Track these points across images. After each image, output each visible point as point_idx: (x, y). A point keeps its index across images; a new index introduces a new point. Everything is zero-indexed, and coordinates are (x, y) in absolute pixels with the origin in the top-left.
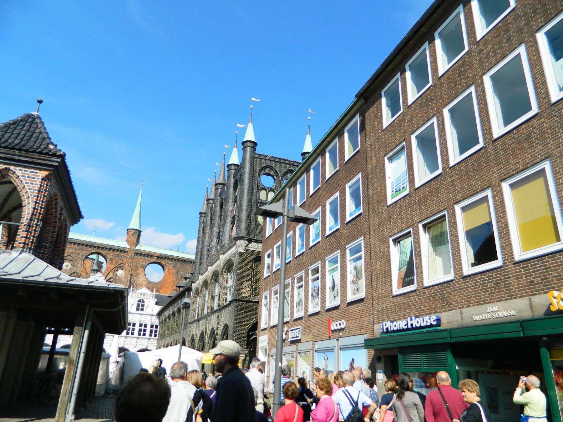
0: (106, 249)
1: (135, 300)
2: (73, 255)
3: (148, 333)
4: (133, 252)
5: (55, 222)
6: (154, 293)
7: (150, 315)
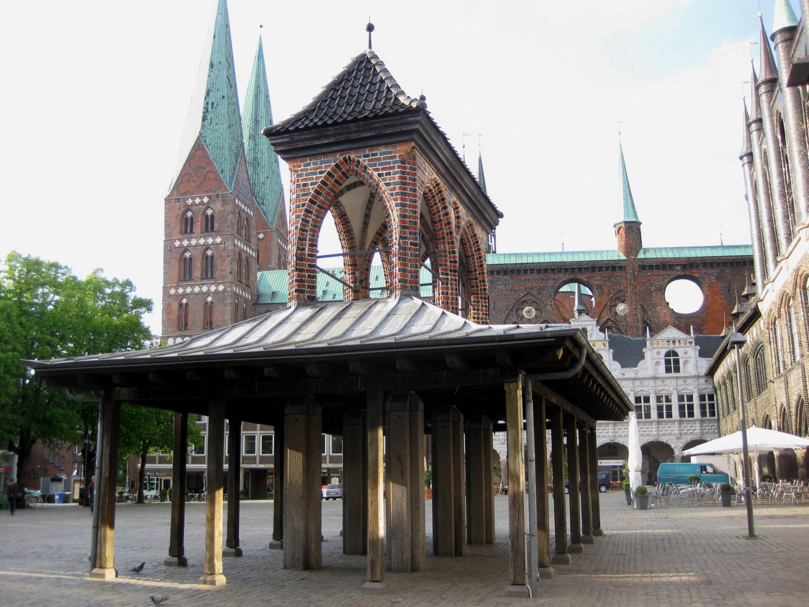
0: (587, 269)
1: (658, 353)
2: (534, 292)
3: (697, 411)
4: (636, 266)
5: (451, 233)
6: (692, 335)
7: (694, 377)
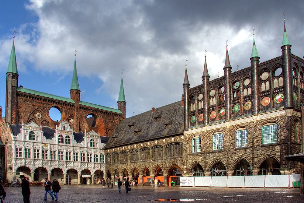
6: (99, 135)
